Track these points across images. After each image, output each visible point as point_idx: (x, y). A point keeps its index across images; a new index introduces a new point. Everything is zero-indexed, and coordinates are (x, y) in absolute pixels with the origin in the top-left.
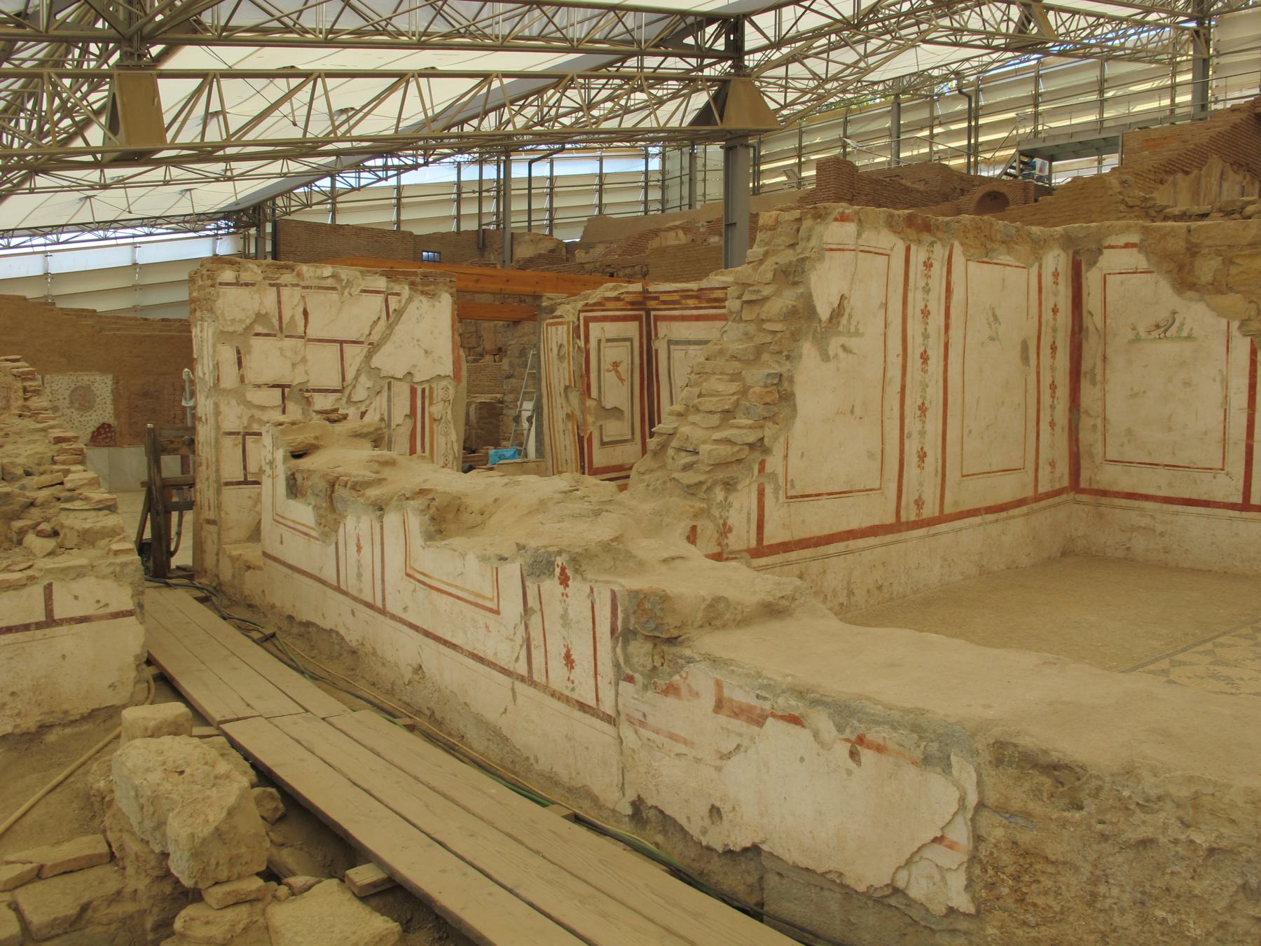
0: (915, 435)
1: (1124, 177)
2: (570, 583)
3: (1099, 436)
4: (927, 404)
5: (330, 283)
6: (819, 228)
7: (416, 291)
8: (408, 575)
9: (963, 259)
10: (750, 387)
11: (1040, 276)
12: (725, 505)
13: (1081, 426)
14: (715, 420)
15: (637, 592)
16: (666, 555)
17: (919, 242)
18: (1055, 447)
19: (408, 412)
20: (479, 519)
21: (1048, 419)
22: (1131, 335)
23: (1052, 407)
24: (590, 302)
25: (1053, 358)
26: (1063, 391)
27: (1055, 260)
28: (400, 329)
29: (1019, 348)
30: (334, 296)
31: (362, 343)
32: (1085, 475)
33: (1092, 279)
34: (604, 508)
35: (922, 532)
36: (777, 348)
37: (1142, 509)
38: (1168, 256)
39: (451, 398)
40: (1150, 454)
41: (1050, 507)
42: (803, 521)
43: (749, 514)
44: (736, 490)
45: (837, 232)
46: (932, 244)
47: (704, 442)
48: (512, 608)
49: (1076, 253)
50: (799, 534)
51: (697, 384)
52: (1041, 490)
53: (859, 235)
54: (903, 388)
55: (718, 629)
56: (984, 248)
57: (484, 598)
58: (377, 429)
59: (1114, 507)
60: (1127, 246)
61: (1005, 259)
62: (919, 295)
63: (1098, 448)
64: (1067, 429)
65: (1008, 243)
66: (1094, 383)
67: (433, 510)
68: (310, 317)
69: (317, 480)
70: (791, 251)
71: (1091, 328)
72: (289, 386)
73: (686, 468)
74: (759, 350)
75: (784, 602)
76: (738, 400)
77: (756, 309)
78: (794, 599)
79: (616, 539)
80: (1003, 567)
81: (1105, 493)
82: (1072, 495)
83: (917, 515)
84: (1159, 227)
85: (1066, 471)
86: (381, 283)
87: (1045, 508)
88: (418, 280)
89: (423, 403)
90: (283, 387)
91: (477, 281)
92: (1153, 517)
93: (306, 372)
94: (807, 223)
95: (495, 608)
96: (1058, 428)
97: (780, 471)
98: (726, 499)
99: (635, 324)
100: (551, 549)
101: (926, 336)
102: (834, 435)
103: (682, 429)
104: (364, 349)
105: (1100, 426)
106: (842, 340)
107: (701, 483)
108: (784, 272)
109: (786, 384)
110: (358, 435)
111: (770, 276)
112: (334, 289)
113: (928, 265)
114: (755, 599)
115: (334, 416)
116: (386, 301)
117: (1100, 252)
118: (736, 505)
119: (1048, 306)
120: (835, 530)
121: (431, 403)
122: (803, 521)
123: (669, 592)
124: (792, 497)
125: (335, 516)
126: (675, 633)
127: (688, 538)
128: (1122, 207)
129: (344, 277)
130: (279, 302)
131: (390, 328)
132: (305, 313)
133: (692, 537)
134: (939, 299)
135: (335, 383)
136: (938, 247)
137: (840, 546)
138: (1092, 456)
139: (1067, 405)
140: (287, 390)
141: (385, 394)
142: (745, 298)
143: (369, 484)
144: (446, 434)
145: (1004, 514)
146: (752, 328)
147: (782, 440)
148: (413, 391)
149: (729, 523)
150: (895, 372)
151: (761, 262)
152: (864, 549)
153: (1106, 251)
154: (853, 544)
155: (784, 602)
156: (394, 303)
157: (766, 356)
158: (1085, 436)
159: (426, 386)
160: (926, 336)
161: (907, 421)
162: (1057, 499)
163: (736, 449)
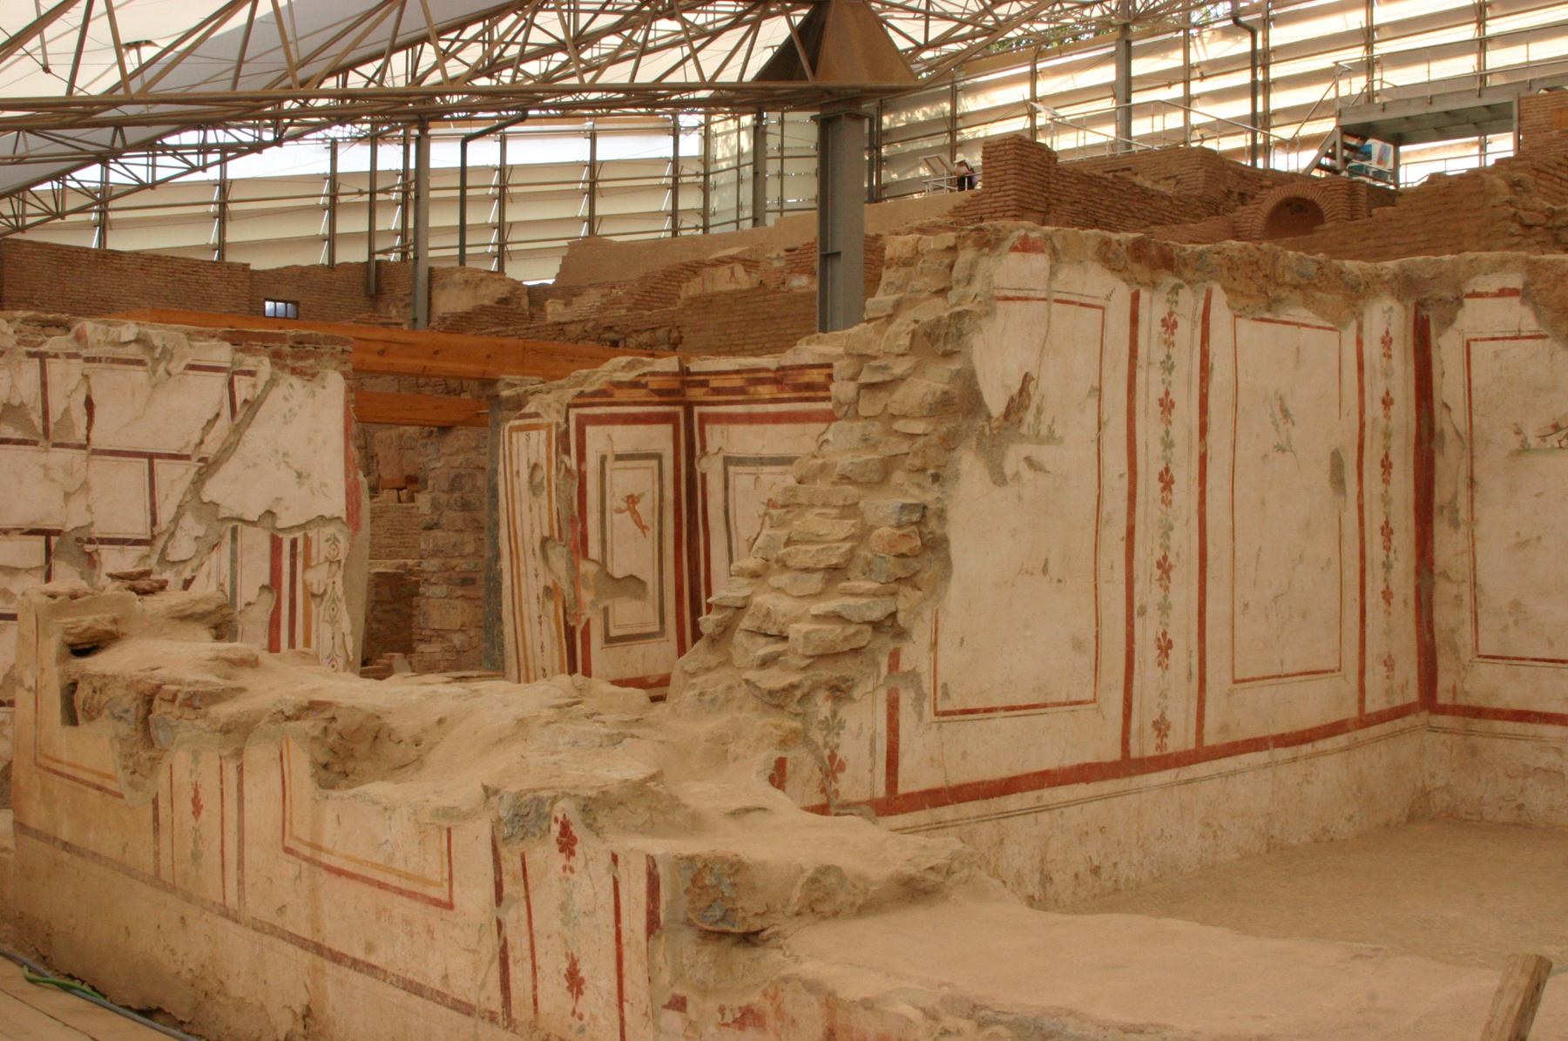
0: (1152, 611)
1: (1518, 175)
2: (577, 848)
3: (1467, 616)
4: (1172, 559)
5: (133, 351)
6: (987, 264)
7: (283, 367)
8: (288, 851)
9: (1228, 315)
10: (873, 528)
11: (1360, 342)
12: (833, 725)
13: (1436, 598)
14: (815, 582)
15: (691, 859)
16: (735, 806)
17: (1154, 285)
18: (1393, 632)
19: (266, 580)
20: (413, 753)
21: (1381, 587)
22: (1514, 443)
23: (1387, 566)
24: (588, 389)
25: (1386, 482)
26: (1405, 538)
27: (1385, 317)
28: (257, 438)
29: (1326, 466)
30: (139, 375)
31: (187, 457)
32: (1444, 682)
33: (1447, 348)
34: (627, 731)
35: (1167, 776)
36: (918, 462)
37: (1538, 738)
39: (342, 557)
40: (1551, 644)
41: (1387, 736)
42: (964, 755)
43: (873, 740)
44: (851, 699)
45: (1014, 270)
46: (1175, 290)
47: (797, 619)
48: (474, 896)
49: (1420, 305)
50: (959, 777)
51: (781, 524)
52: (1371, 707)
53: (1053, 274)
54: (1131, 531)
55: (825, 918)
56: (1262, 293)
57: (427, 883)
58: (220, 607)
59: (1495, 735)
60: (1502, 293)
61: (1302, 314)
62: (1156, 375)
63: (1465, 636)
64: (1412, 603)
65: (1306, 288)
66: (1455, 524)
67: (332, 738)
68: (97, 412)
69: (120, 692)
70: (939, 301)
71: (1448, 431)
72: (58, 533)
73: (765, 663)
74: (887, 467)
75: (932, 877)
76: (852, 550)
77: (882, 396)
78: (950, 872)
79: (653, 777)
80: (1306, 838)
81: (1478, 712)
82: (1424, 715)
83: (1158, 747)
84: (1552, 263)
85: (1413, 674)
86: (222, 353)
87: (1378, 739)
88: (286, 349)
89: (293, 565)
90: (47, 534)
91: (381, 353)
92: (1559, 751)
93: (89, 509)
94: (966, 255)
95: (445, 898)
96: (1397, 601)
97: (925, 668)
98: (834, 714)
99: (667, 429)
100: (543, 794)
101: (1168, 444)
102: (1016, 615)
103: (758, 599)
104: (192, 467)
105: (1467, 597)
106: (1028, 449)
107: (793, 687)
108: (929, 335)
109: (933, 524)
110: (185, 617)
111: (904, 342)
112: (140, 363)
113: (1169, 325)
114: (887, 871)
115: (143, 584)
116: (231, 384)
117: (1458, 302)
118: (852, 724)
119: (1374, 393)
120: (1019, 770)
121: (307, 566)
122: (964, 755)
123: (745, 858)
124: (945, 714)
125: (152, 753)
126: (756, 924)
127: (772, 780)
128: (1515, 228)
129: (157, 342)
130: (44, 385)
131: (238, 431)
132: (89, 405)
133: (778, 776)
134: (1190, 382)
135: (141, 530)
136: (1185, 295)
137: (1029, 798)
138: (1455, 649)
139: (1412, 563)
140: (54, 540)
141: (226, 548)
142: (865, 378)
143: (215, 697)
144: (333, 621)
145: (1306, 748)
146: (875, 429)
147: (928, 615)
148: (276, 545)
149: (841, 754)
150: (1116, 503)
151: (890, 318)
152: (1068, 804)
153: (1468, 302)
154: (1050, 795)
155: (932, 877)
156: (243, 389)
157: (898, 477)
158: (1444, 616)
159: (299, 535)
160: (1168, 444)
161: (1137, 588)
162: (1399, 723)
163: (851, 630)
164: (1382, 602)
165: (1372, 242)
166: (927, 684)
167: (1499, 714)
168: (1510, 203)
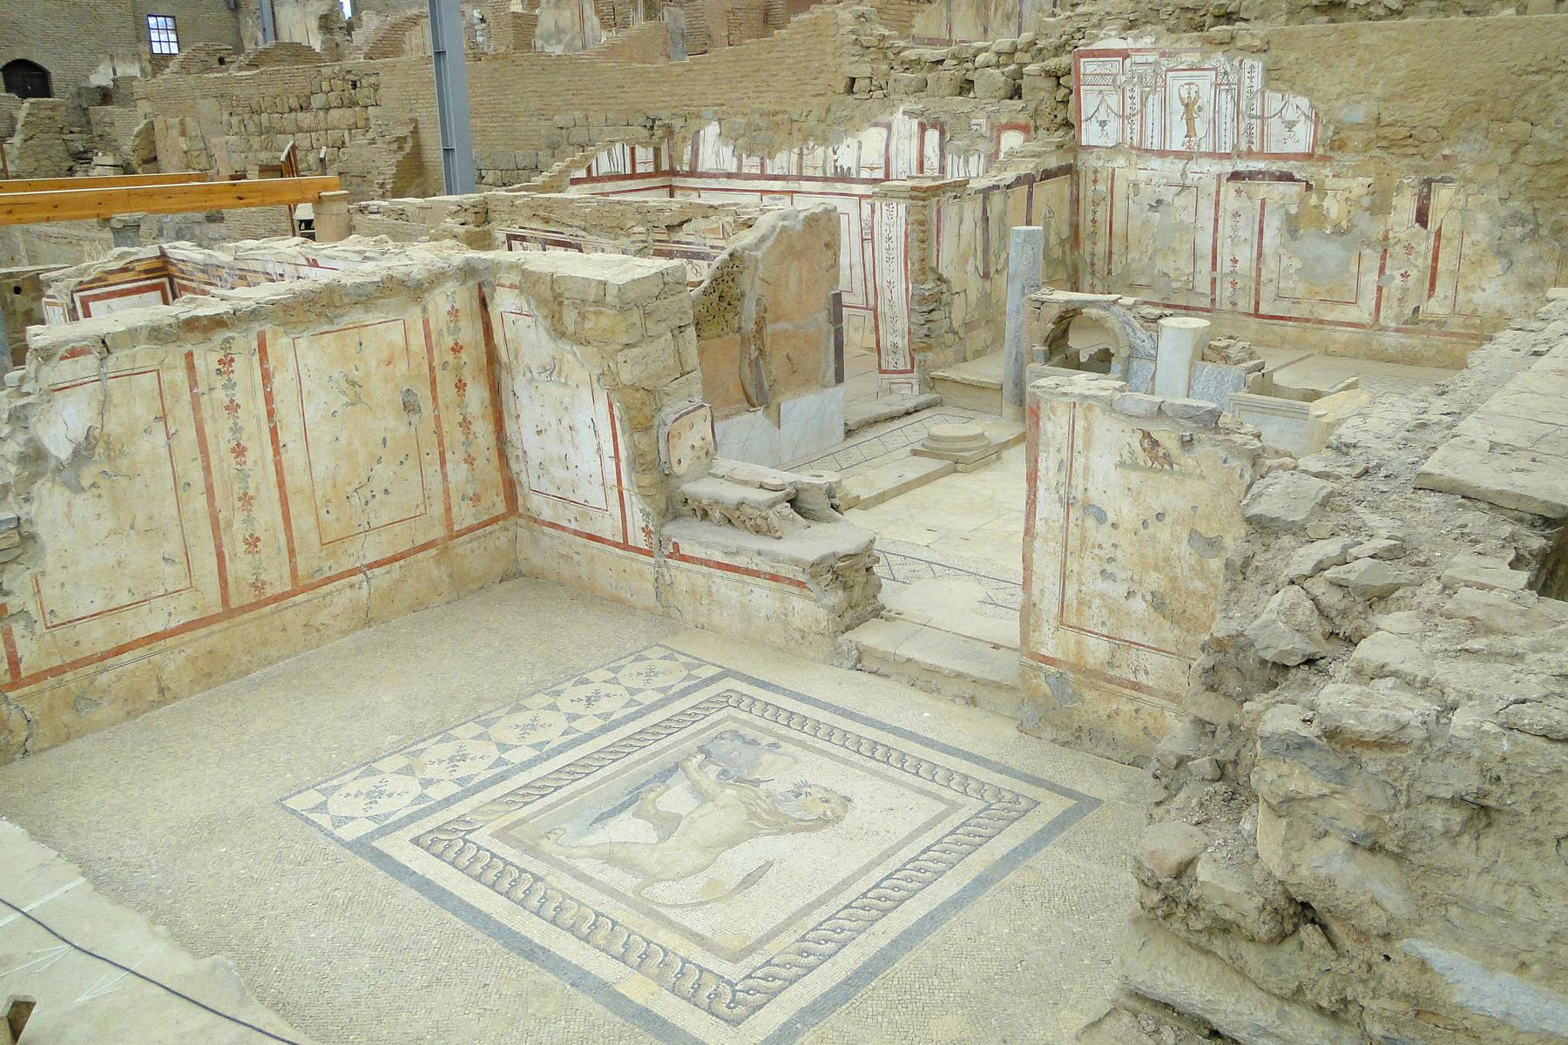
4: (251, 492)
32: (520, 501)
38: (541, 302)
49: (480, 286)
52: (456, 528)
91: (10, 212)
96: (480, 462)
109: (25, 528)
160: (236, 429)
164: (465, 466)
165: (774, 54)
166: (35, 614)
167: (543, 523)
168: (853, 32)
